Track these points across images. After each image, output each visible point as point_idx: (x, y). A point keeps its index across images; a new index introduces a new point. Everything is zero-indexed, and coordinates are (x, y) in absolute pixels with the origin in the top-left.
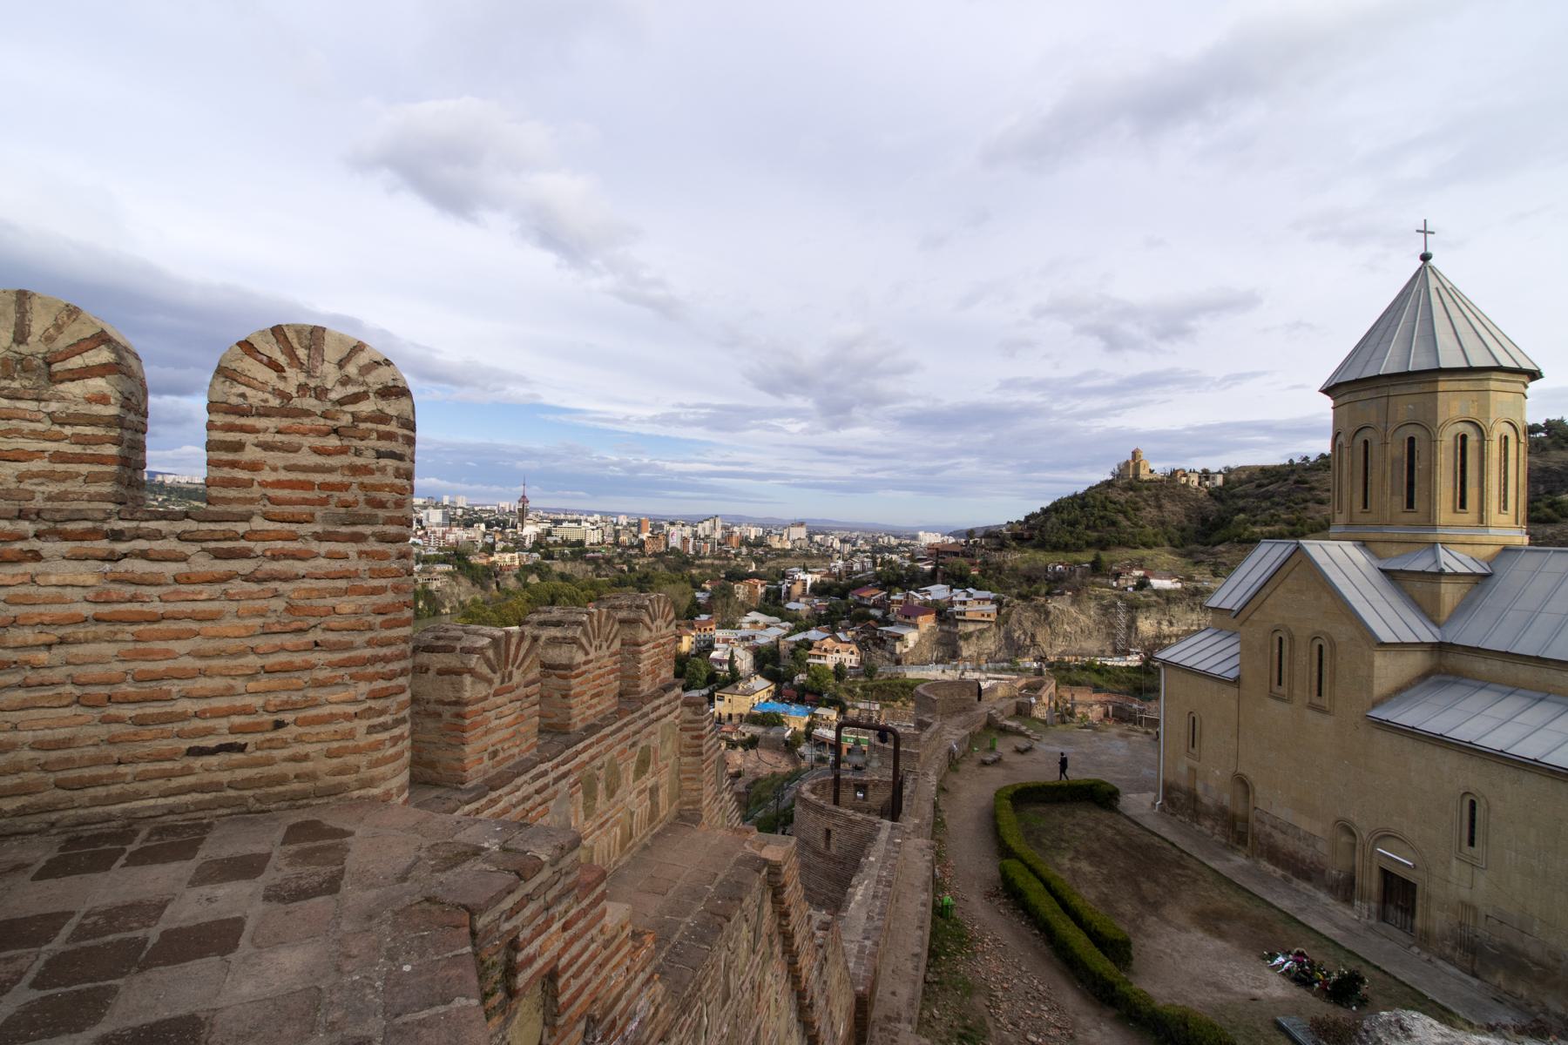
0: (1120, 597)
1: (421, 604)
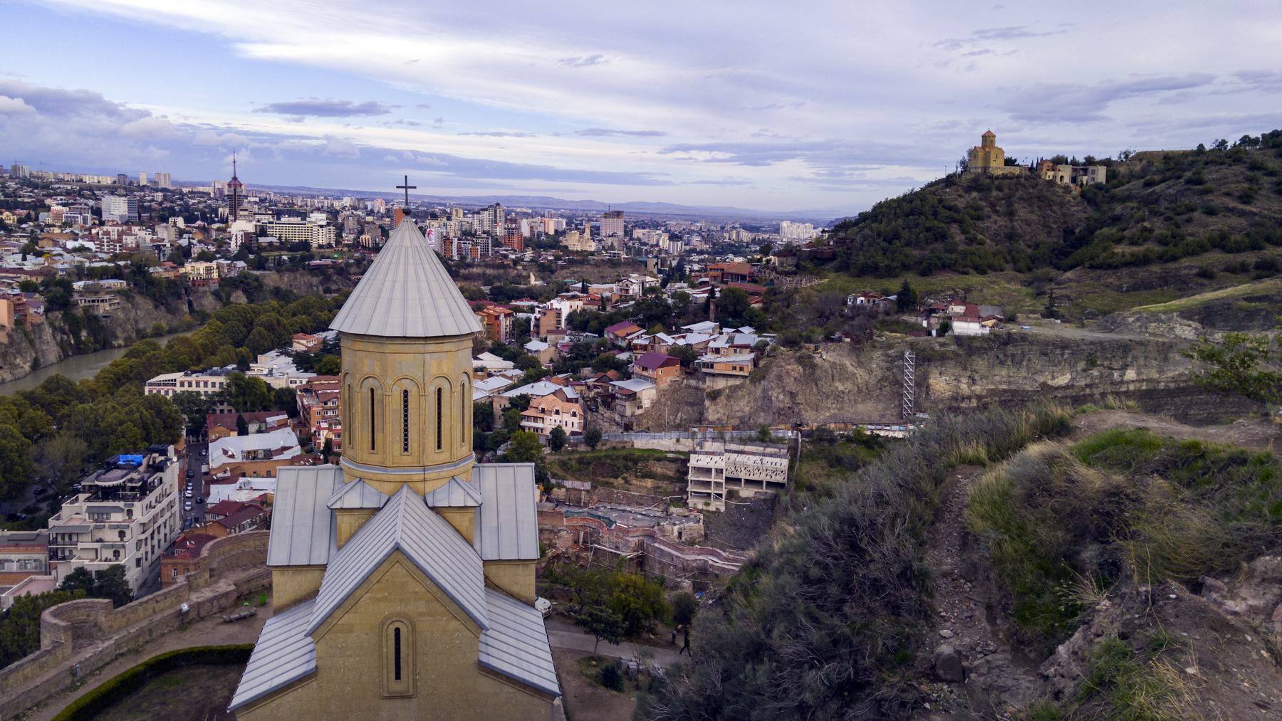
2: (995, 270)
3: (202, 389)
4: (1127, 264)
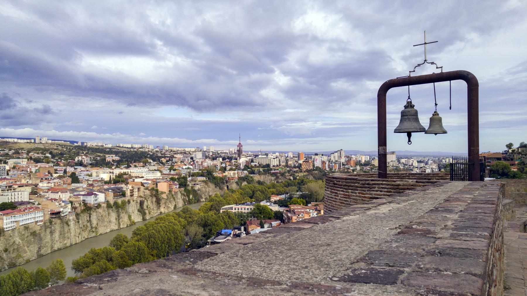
1: (191, 196)
3: (243, 211)
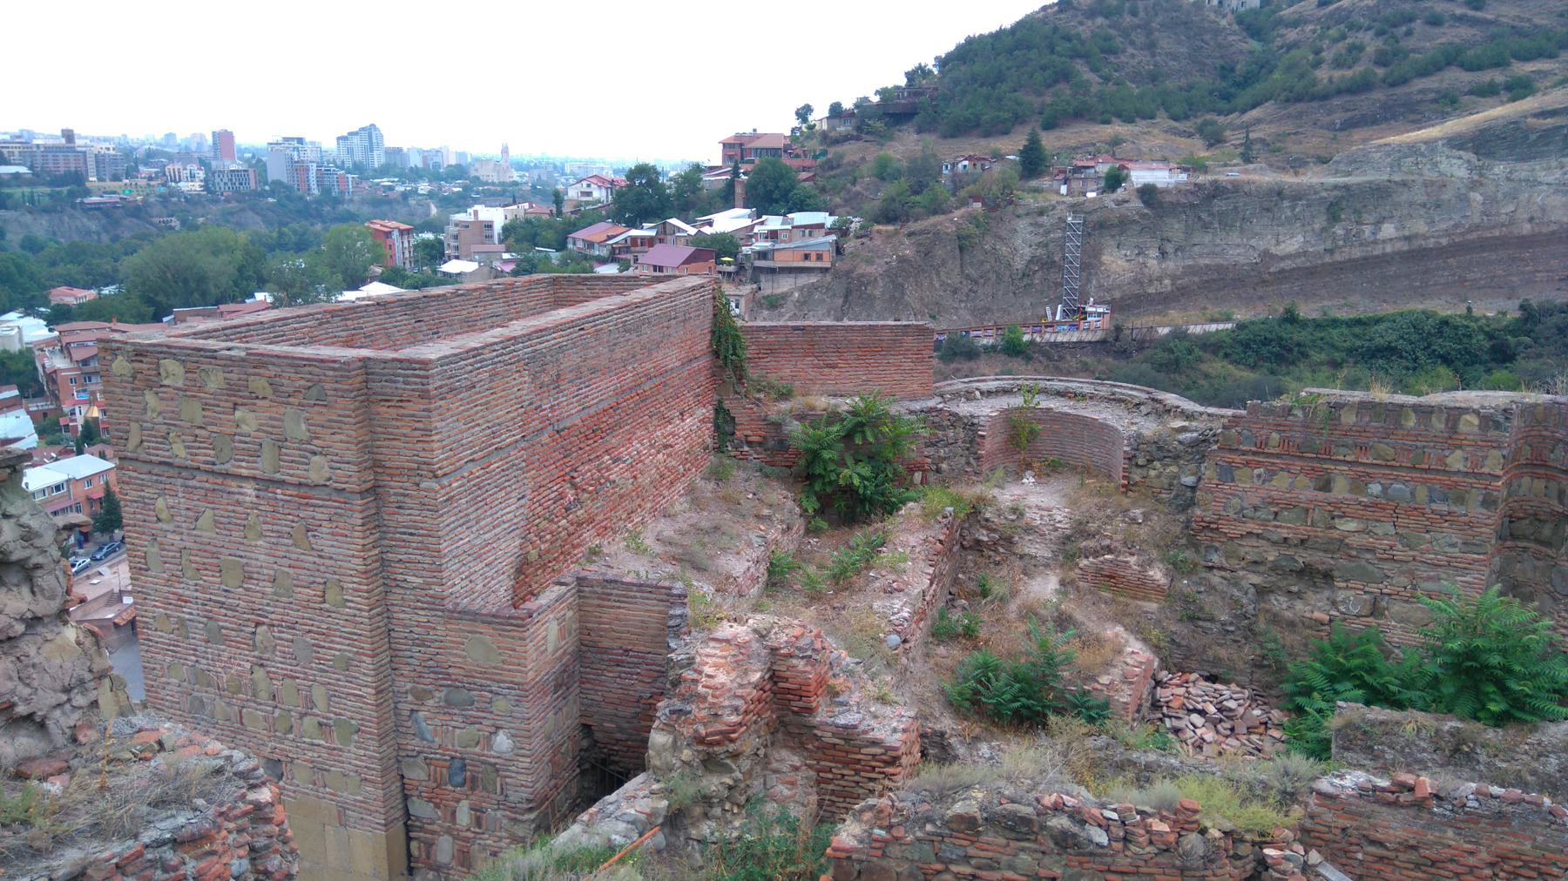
0: (1075, 209)
2: (1144, 118)
4: (1339, 92)
